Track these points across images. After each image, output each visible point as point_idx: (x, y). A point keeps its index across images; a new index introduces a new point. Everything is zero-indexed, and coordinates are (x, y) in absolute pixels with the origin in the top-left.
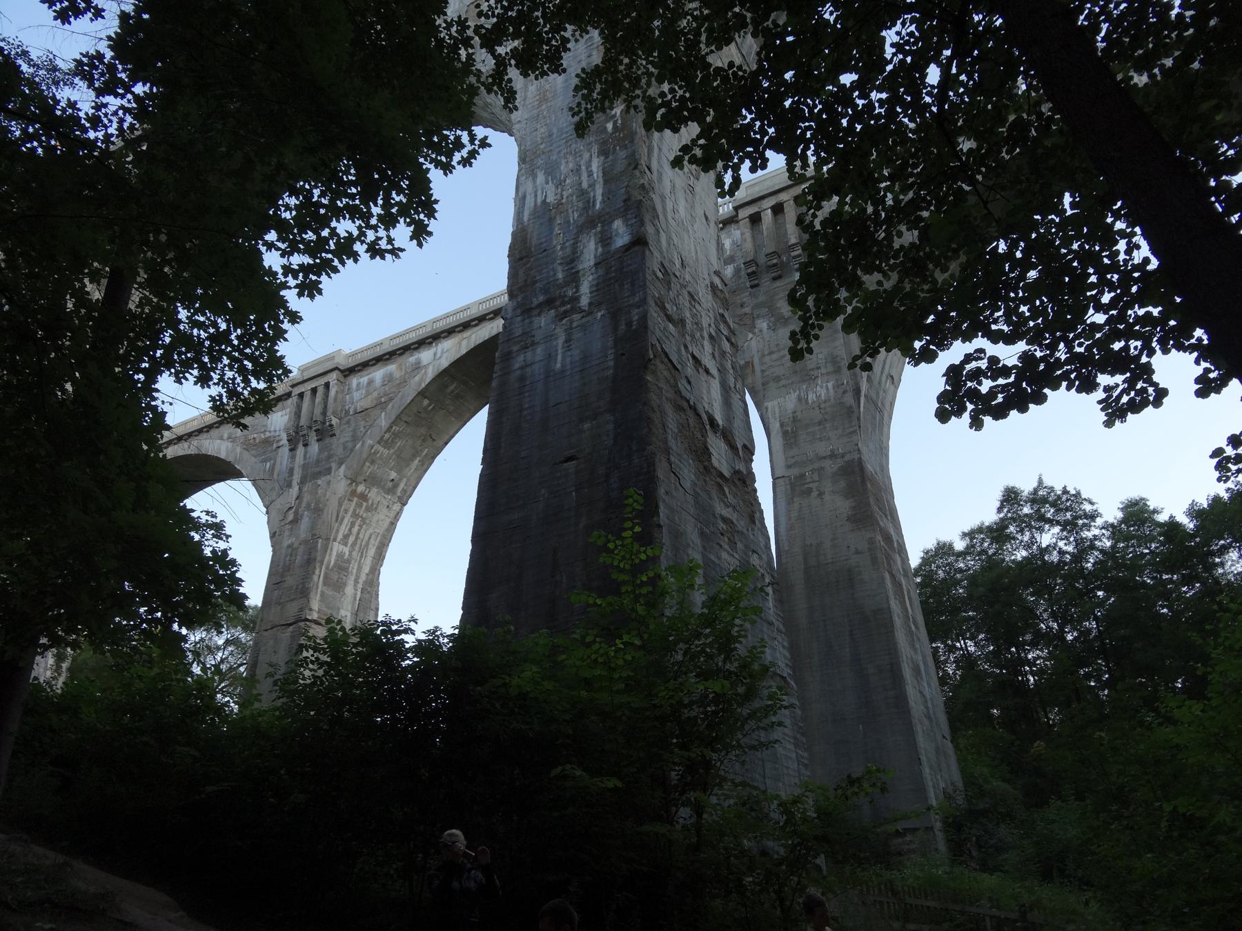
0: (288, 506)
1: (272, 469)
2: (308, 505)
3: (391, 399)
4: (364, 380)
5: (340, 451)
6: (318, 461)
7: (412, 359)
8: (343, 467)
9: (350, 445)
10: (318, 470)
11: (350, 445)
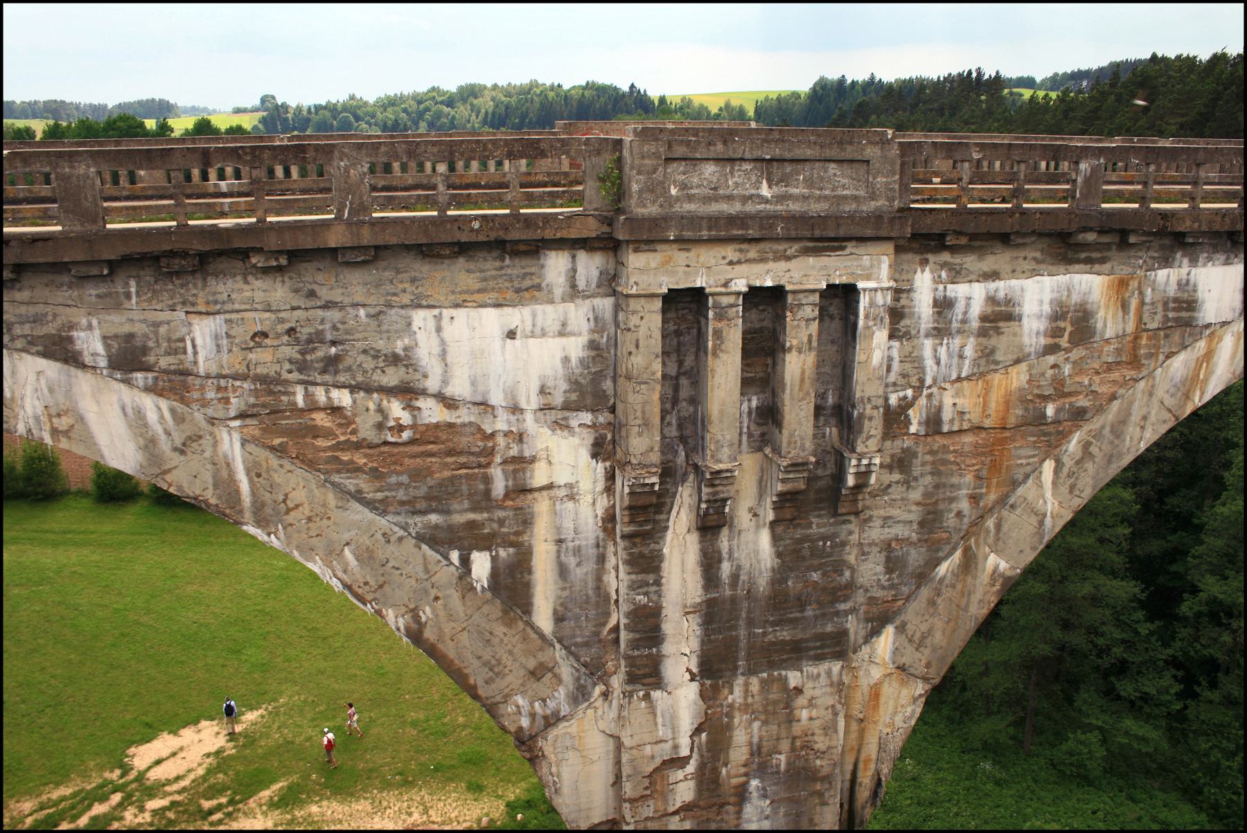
0: (665, 751)
1: (512, 588)
2: (757, 751)
3: (1079, 415)
4: (972, 296)
5: (871, 571)
6: (780, 602)
7: (1167, 278)
8: (889, 630)
9: (915, 557)
10: (785, 634)
11: (915, 557)
